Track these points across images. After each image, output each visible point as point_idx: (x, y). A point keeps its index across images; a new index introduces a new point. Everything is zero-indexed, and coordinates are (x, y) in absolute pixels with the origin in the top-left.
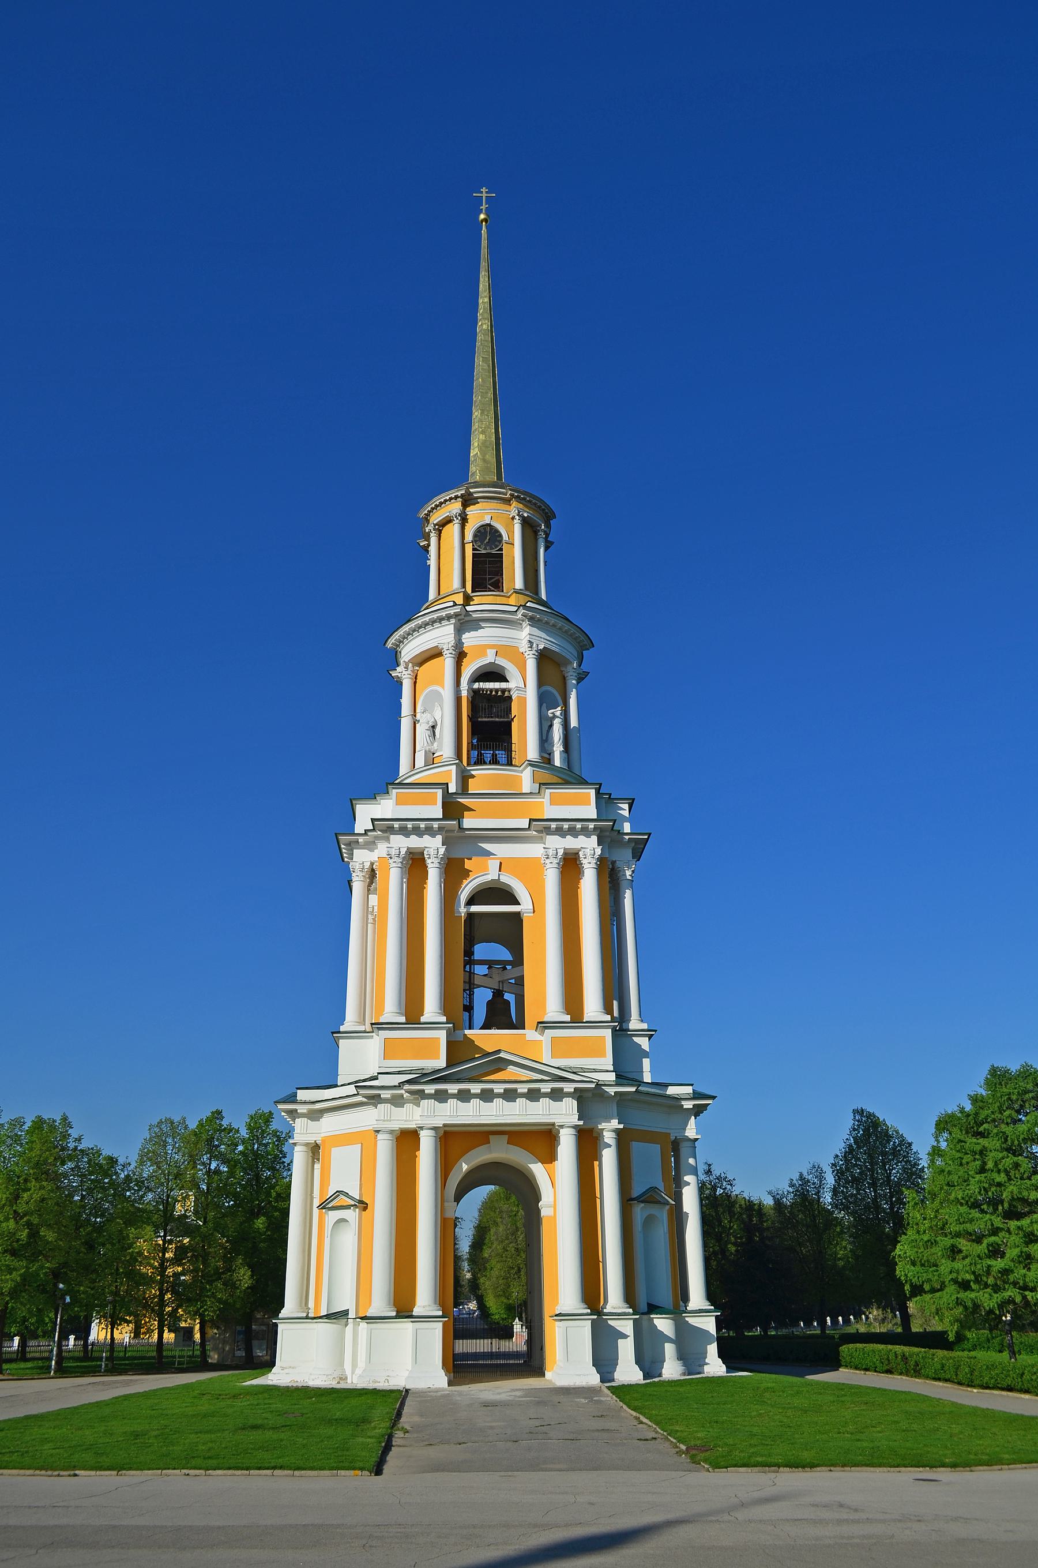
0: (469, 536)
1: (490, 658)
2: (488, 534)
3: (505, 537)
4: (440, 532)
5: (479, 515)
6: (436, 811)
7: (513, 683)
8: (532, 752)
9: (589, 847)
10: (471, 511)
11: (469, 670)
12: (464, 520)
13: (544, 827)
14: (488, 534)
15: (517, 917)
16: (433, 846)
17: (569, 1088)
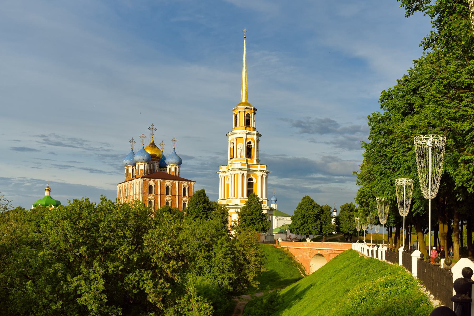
0: (245, 116)
1: (250, 140)
2: (248, 115)
3: (251, 116)
4: (239, 112)
5: (248, 111)
6: (246, 167)
7: (252, 144)
8: (255, 157)
9: (265, 174)
10: (246, 110)
11: (247, 142)
12: (245, 112)
13: (260, 171)
14: (248, 115)
15: (253, 183)
16: (246, 173)
17: (267, 209)
